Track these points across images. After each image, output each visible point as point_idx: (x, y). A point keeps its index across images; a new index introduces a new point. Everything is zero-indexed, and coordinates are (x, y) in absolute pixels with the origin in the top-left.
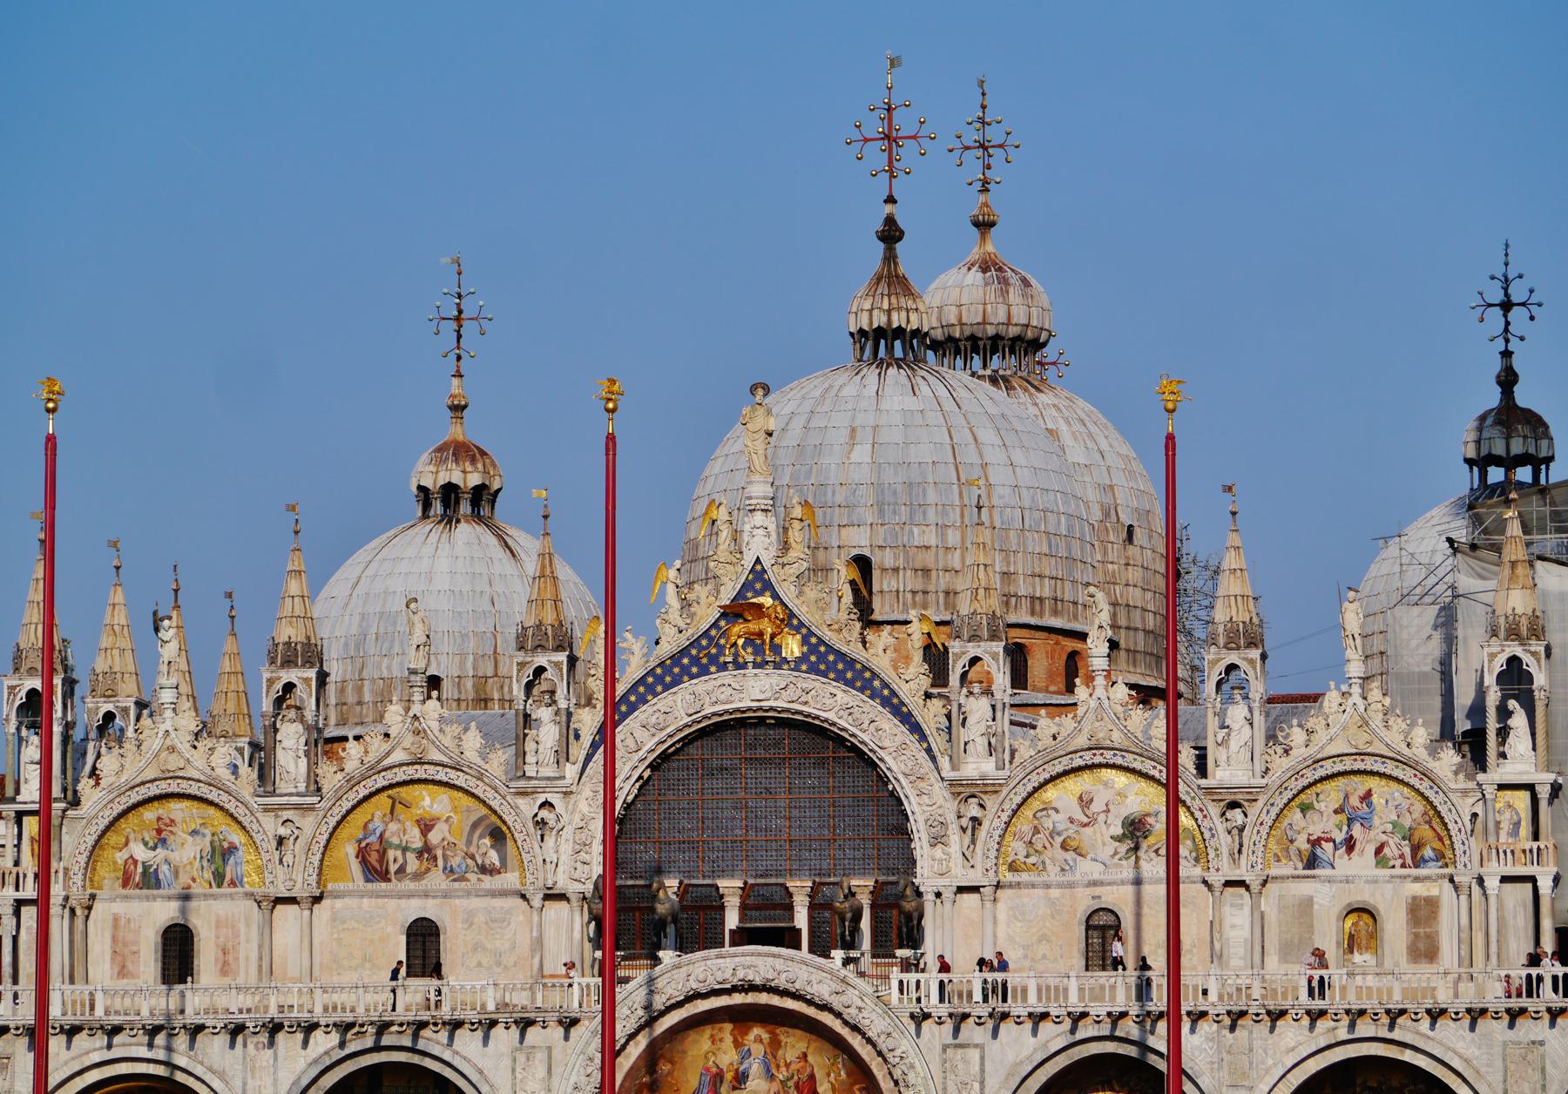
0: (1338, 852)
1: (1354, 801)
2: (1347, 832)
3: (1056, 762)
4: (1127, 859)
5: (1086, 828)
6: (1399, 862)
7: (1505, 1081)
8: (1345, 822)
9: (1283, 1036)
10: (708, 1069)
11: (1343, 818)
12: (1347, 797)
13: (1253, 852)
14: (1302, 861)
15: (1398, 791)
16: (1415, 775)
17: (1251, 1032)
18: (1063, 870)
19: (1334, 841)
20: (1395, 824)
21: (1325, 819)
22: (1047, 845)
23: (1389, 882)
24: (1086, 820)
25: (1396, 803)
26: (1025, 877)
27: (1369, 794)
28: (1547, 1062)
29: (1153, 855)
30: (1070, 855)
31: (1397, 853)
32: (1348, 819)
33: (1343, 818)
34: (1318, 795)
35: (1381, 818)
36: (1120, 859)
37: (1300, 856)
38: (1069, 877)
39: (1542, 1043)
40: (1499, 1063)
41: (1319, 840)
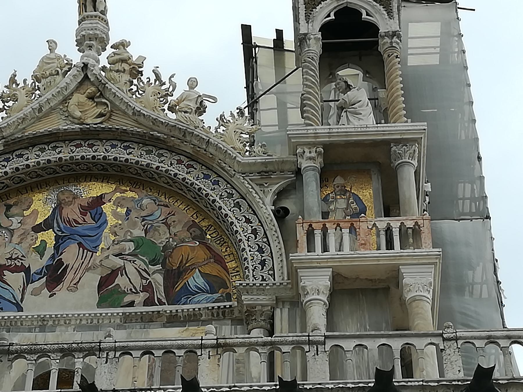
0: (31, 287)
2: (53, 257)
6: (142, 296)
19: (27, 270)
23: (119, 327)
25: (144, 214)
32: (57, 238)
35: (116, 235)
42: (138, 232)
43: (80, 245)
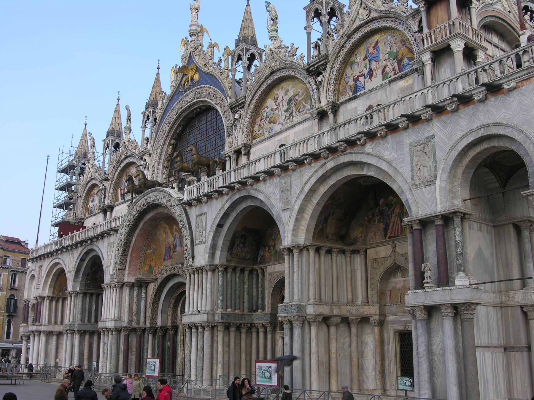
1: (371, 50)
3: (262, 85)
4: (289, 118)
5: (277, 111)
6: (393, 72)
7: (412, 170)
8: (368, 63)
9: (304, 175)
10: (166, 245)
11: (367, 61)
12: (368, 50)
13: (328, 94)
14: (352, 91)
15: (389, 35)
16: (392, 21)
17: (291, 177)
18: (269, 132)
19: (363, 75)
20: (389, 54)
21: (360, 65)
22: (265, 124)
24: (276, 107)
26: (258, 140)
27: (377, 43)
28: (437, 149)
29: (297, 113)
30: (271, 125)
31: (391, 68)
32: (369, 61)
33: (367, 61)
34: (356, 55)
36: (287, 120)
37: (351, 89)
38: (271, 134)
39: (433, 137)
40: (408, 159)
41: (358, 76)
42: (389, 50)
43: (375, 61)
